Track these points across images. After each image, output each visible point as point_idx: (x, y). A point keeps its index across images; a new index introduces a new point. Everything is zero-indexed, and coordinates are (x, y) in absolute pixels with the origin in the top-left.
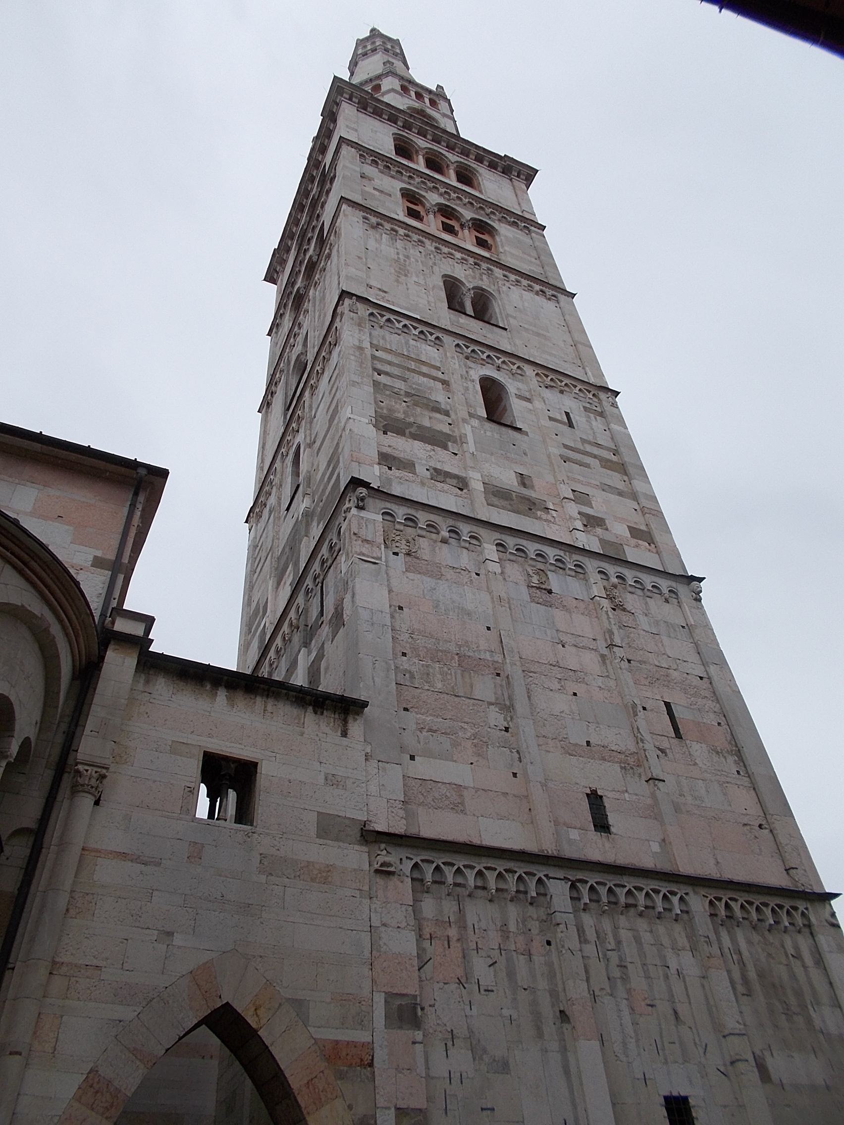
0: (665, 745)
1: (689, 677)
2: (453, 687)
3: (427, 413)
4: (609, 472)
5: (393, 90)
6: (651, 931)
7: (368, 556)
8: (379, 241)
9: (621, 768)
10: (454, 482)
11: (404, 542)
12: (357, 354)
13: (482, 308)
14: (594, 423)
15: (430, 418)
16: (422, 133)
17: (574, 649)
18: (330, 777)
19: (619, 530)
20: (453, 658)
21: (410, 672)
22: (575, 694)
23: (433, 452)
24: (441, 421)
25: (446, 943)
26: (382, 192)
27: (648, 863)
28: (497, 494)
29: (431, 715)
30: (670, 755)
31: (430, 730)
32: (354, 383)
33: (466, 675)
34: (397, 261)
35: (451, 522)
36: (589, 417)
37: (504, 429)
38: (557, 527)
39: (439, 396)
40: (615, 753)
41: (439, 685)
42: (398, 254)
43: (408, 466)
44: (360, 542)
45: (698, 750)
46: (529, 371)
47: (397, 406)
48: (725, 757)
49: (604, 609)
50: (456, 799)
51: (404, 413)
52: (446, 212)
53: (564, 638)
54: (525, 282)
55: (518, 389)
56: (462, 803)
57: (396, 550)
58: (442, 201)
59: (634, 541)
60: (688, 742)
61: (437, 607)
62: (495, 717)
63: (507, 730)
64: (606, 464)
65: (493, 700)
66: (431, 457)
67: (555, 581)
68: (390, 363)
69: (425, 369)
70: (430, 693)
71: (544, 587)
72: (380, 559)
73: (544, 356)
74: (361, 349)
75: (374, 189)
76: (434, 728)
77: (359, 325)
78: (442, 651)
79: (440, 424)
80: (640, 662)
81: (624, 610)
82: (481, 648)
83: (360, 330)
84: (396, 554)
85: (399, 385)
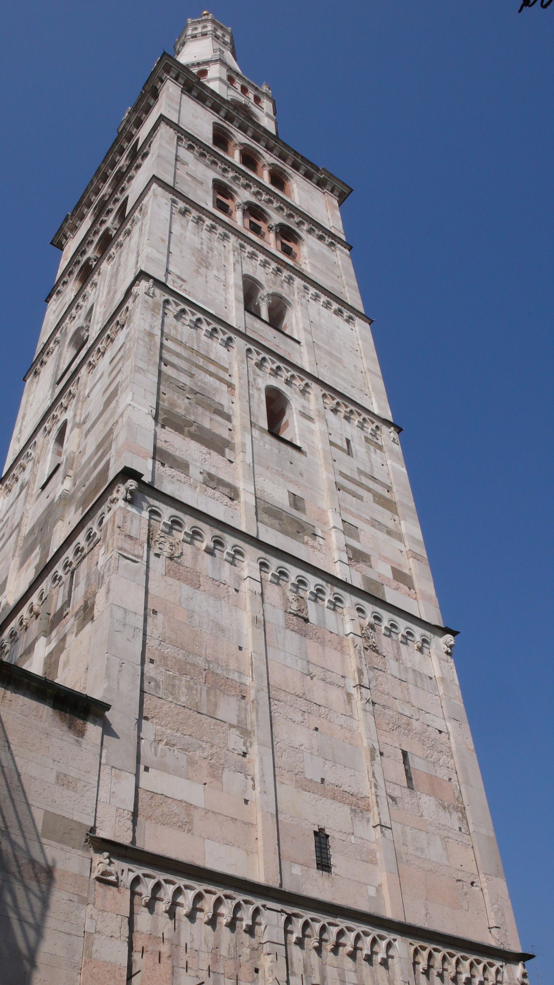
0: (396, 793)
2: (197, 703)
4: (381, 508)
6: (356, 971)
7: (129, 553)
8: (184, 227)
9: (352, 810)
10: (226, 491)
12: (147, 339)
14: (373, 455)
15: (211, 420)
16: (243, 129)
17: (322, 683)
19: (382, 570)
20: (201, 673)
21: (155, 681)
22: (316, 729)
23: (208, 456)
25: (157, 957)
26: (194, 178)
27: (363, 906)
28: (265, 510)
29: (171, 729)
30: (400, 805)
32: (138, 370)
34: (200, 251)
35: (218, 532)
37: (283, 446)
38: (323, 556)
39: (223, 398)
40: (346, 795)
41: (183, 699)
43: (182, 466)
44: (123, 537)
45: (427, 803)
46: (315, 390)
48: (450, 813)
50: (185, 818)
51: (186, 409)
52: (253, 211)
53: (314, 670)
54: (324, 298)
55: (303, 407)
56: (190, 822)
58: (253, 199)
59: (395, 583)
61: (191, 617)
62: (235, 741)
65: (235, 722)
67: (312, 611)
68: (178, 355)
69: (212, 368)
72: (142, 557)
74: (151, 335)
75: (188, 174)
77: (153, 310)
78: (190, 664)
79: (219, 427)
80: (384, 706)
81: (377, 651)
83: (153, 315)
84: (157, 555)
85: (184, 379)
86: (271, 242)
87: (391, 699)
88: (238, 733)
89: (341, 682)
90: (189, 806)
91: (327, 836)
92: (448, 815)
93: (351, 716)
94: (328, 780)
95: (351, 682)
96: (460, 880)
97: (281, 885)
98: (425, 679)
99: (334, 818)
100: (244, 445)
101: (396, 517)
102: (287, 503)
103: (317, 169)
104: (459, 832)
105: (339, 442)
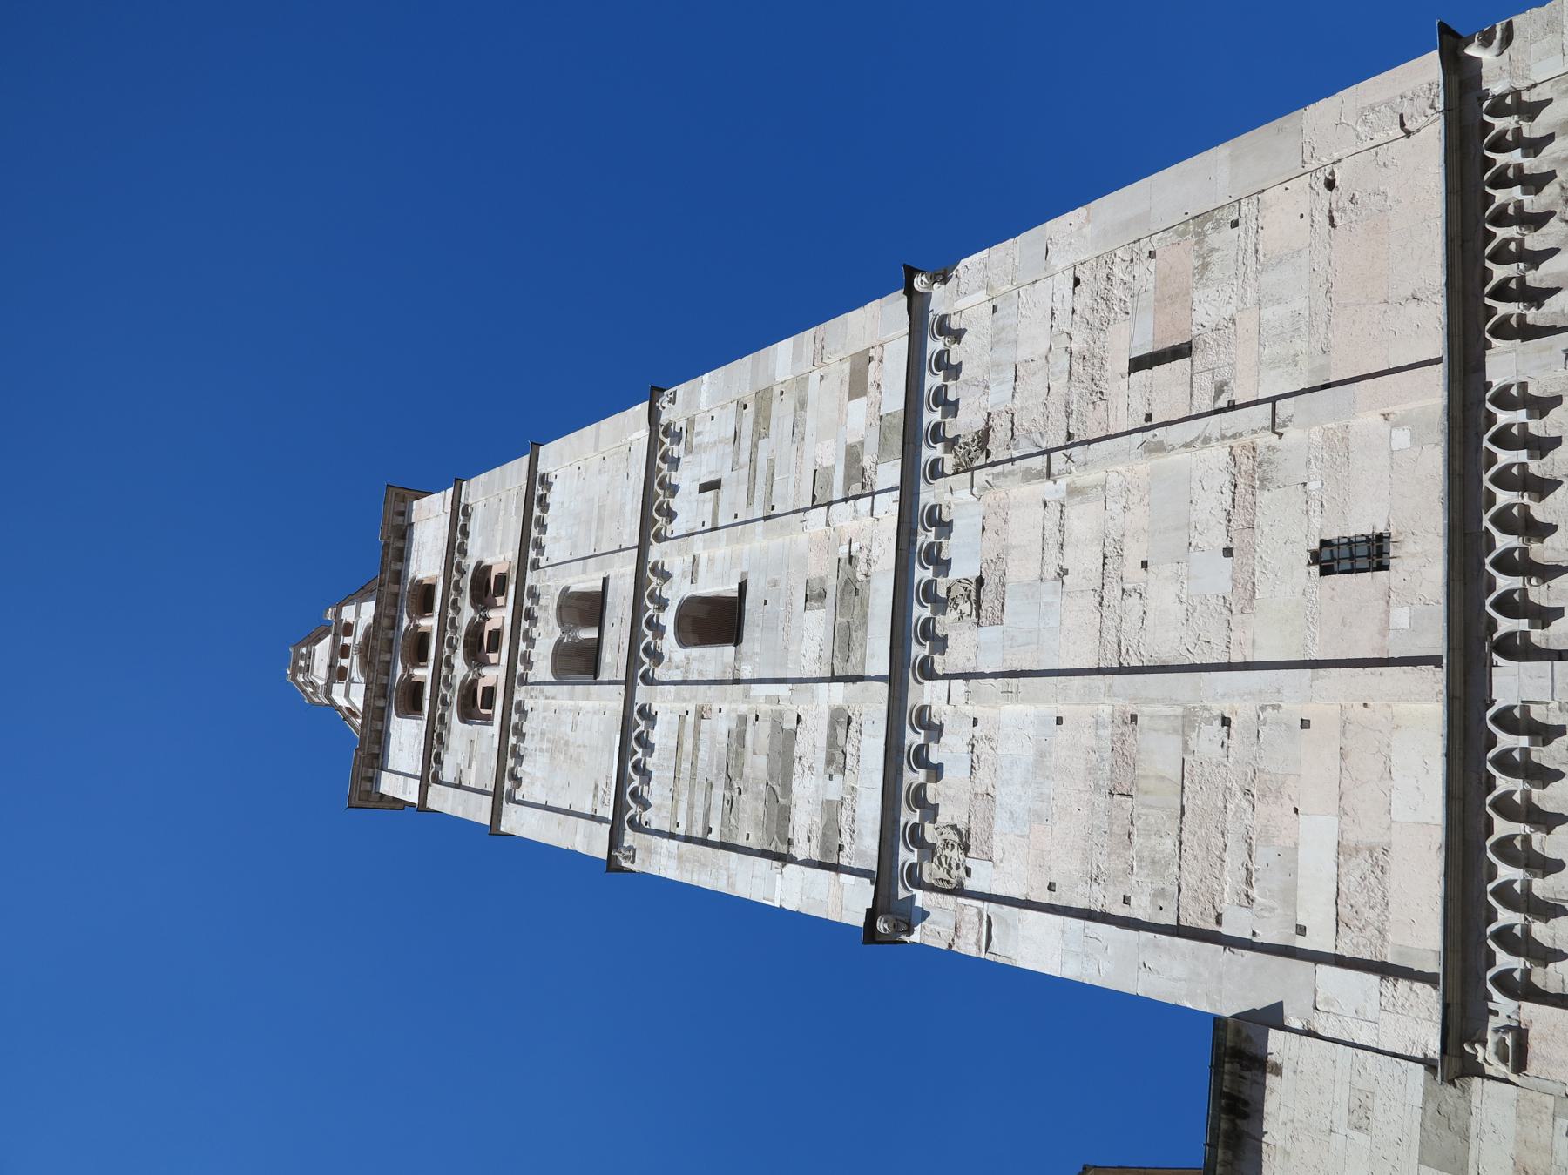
1: (1078, 309)
3: (749, 757)
4: (773, 423)
5: (347, 695)
7: (980, 933)
9: (1263, 487)
10: (841, 732)
11: (947, 852)
13: (587, 608)
18: (1354, 1119)
21: (1155, 896)
22: (1144, 564)
23: (804, 761)
24: (755, 734)
30: (1225, 374)
31: (1249, 882)
33: (1143, 784)
36: (699, 446)
39: (720, 726)
41: (1169, 844)
42: (541, 750)
43: (832, 810)
48: (1212, 250)
49: (990, 479)
57: (962, 869)
58: (460, 651)
60: (1196, 333)
63: (1226, 722)
65: (1178, 740)
68: (691, 807)
69: (688, 746)
71: (973, 594)
76: (1244, 872)
80: (1069, 415)
86: (500, 617)
87: (1051, 398)
89: (1054, 509)
91: (1324, 543)
92: (1216, 255)
93: (1104, 487)
94: (1225, 543)
95: (1053, 490)
96: (1332, 219)
97: (1434, 661)
100: (768, 699)
101: (777, 391)
103: (387, 545)
105: (709, 507)
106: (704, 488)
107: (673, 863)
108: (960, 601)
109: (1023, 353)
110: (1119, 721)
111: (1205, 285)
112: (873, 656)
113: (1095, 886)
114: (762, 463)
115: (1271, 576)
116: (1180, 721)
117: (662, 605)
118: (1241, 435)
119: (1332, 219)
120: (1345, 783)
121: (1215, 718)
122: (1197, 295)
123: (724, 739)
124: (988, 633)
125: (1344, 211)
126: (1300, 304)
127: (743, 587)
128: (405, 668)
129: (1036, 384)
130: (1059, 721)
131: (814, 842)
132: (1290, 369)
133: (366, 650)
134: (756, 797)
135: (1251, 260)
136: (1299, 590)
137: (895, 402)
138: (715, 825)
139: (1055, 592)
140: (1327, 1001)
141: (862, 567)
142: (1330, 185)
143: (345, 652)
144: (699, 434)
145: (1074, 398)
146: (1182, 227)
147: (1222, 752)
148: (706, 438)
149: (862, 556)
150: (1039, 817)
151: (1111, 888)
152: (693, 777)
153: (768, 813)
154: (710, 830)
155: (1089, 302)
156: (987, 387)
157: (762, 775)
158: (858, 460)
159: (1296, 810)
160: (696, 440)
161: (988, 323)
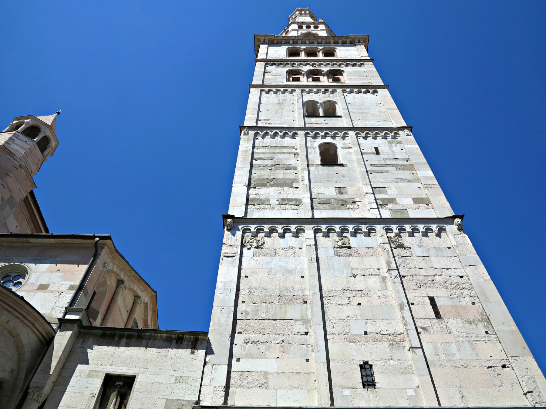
1: (451, 278)
3: (282, 172)
4: (402, 172)
5: (293, 30)
7: (229, 253)
9: (390, 344)
10: (293, 203)
11: (255, 241)
12: (244, 154)
13: (330, 111)
18: (179, 378)
22: (359, 304)
24: (291, 173)
30: (430, 330)
31: (253, 342)
33: (283, 306)
36: (391, 146)
39: (292, 161)
41: (264, 316)
42: (279, 100)
43: (266, 201)
47: (265, 173)
48: (476, 325)
57: (250, 247)
58: (312, 68)
60: (445, 320)
63: (306, 334)
64: (400, 168)
65: (299, 318)
66: (280, 193)
68: (264, 153)
69: (285, 150)
70: (257, 321)
71: (345, 246)
73: (364, 122)
76: (256, 341)
78: (269, 296)
79: (290, 175)
80: (412, 276)
82: (296, 289)
86: (325, 81)
87: (418, 270)
88: (301, 323)
89: (377, 272)
90: (266, 373)
91: (371, 366)
92: (475, 326)
93: (386, 289)
94: (369, 331)
95: (384, 271)
96: (491, 367)
97: (332, 403)
98: (444, 250)
99: (374, 354)
100: (303, 177)
101: (414, 172)
102: (335, 193)
103: (347, 37)
104: (486, 335)
105: (370, 151)
106: (376, 149)
107: (244, 149)
108: (342, 241)
109: (434, 259)
110: (304, 297)
111: (463, 323)
112: (321, 212)
113: (248, 291)
114: (387, 169)
115: (358, 348)
116: (305, 318)
117: (333, 137)
118: (408, 337)
119: (491, 367)
120: (288, 374)
121: (307, 330)
122: (459, 320)
123: (288, 162)
124: (331, 251)
125: (494, 371)
126: (458, 356)
127: (342, 165)
128: (304, 49)
129: (422, 264)
130: (303, 277)
131: (255, 196)
132: (434, 353)
133: (309, 35)
134: (269, 175)
135: (474, 339)
136: (354, 358)
137: (412, 214)
138: (259, 162)
139: (347, 274)
140: (216, 369)
141: (352, 206)
142: (504, 366)
143: (308, 27)
144: (396, 145)
145: (418, 278)
146: (485, 314)
147: (296, 333)
148: (394, 148)
149: (356, 206)
150: (270, 271)
151: (247, 297)
152: (274, 153)
153: (264, 180)
154: (256, 160)
155: (454, 282)
156: (420, 247)
157: (277, 177)
158: (390, 203)
159: (278, 358)
160: (393, 145)
161: (444, 246)
